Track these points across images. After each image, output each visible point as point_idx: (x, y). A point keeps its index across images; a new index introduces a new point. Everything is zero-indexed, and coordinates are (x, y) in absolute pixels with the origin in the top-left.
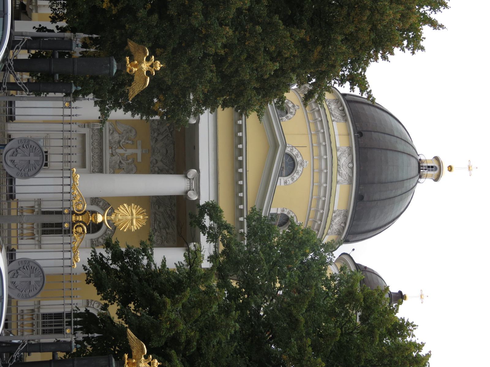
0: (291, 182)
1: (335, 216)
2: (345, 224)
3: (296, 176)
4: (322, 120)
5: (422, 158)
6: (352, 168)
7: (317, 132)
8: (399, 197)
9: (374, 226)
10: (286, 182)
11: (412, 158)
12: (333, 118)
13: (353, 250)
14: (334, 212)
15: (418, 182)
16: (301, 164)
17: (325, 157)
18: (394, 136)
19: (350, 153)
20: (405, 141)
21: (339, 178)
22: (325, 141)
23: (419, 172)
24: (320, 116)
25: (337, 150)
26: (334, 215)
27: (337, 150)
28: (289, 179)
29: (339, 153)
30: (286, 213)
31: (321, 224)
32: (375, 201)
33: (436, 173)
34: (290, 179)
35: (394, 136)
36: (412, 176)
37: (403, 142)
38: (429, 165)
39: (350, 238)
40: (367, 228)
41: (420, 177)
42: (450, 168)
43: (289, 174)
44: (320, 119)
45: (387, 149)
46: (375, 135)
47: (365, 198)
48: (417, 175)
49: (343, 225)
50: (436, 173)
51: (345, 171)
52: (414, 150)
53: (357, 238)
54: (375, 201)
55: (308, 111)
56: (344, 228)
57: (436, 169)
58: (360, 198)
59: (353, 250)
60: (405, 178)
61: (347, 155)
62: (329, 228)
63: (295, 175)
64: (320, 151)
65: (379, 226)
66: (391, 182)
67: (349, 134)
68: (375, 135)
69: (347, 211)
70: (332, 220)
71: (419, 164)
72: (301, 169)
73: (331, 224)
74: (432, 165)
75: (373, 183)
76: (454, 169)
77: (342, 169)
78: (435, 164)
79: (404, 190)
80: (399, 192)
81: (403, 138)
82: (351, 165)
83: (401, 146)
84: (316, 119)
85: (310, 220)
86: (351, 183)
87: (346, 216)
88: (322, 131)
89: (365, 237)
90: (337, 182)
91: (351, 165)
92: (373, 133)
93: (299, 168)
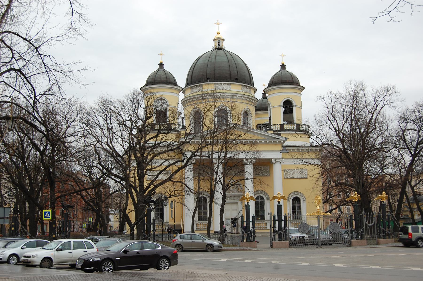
2: (247, 86)
6: (224, 83)
19: (218, 84)
21: (228, 89)
26: (243, 91)
31: (248, 98)
42: (218, 33)
46: (208, 72)
47: (237, 77)
49: (248, 87)
58: (237, 80)
66: (229, 65)
67: (208, 84)
68: (208, 72)
69: (242, 85)
70: (246, 92)
75: (230, 74)
78: (217, 41)
79: (232, 59)
82: (223, 84)
86: (230, 84)
90: (230, 90)
92: (207, 73)
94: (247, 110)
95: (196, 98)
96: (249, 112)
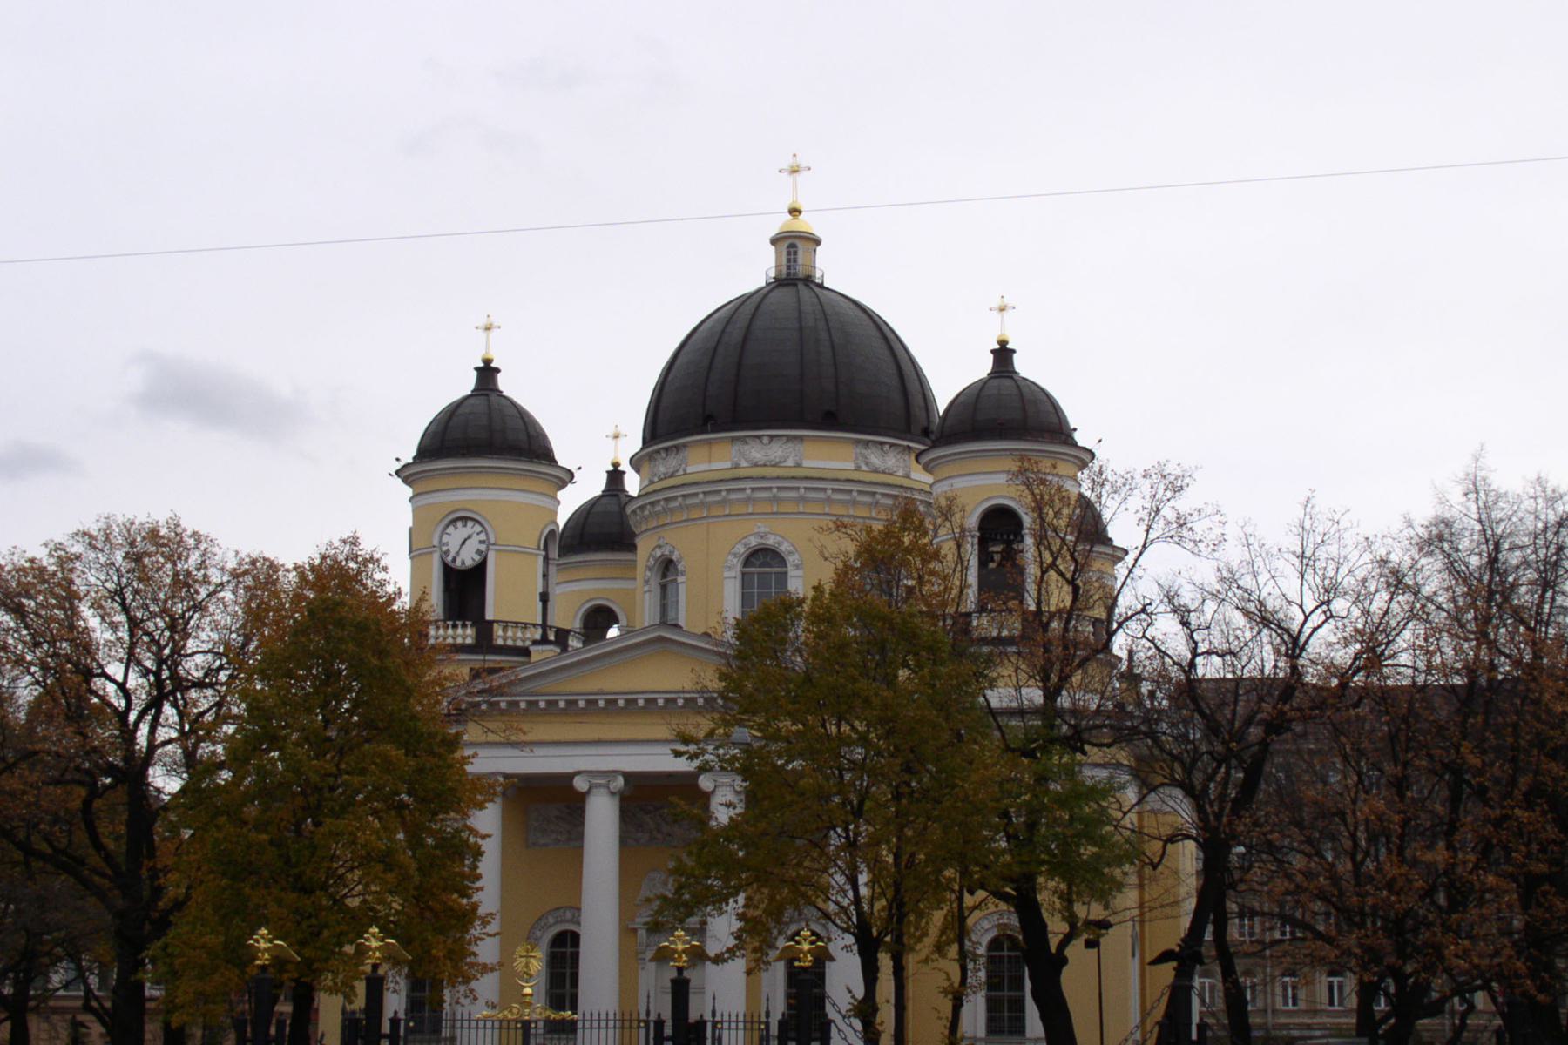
1: (867, 464)
2: (882, 443)
3: (784, 548)
5: (772, 274)
6: (772, 437)
7: (702, 504)
10: (797, 567)
11: (767, 301)
12: (681, 472)
16: (762, 537)
17: (748, 492)
19: (743, 440)
24: (675, 498)
26: (864, 468)
27: (737, 466)
28: (791, 560)
29: (744, 464)
33: (799, 244)
34: (791, 559)
37: (729, 328)
44: (680, 499)
45: (739, 364)
49: (886, 447)
51: (776, 451)
56: (892, 445)
57: (793, 246)
61: (746, 447)
63: (783, 548)
67: (709, 442)
69: (858, 442)
73: (884, 472)
77: (772, 457)
83: (736, 334)
86: (801, 438)
87: (867, 444)
91: (765, 440)
93: (770, 541)
95: (662, 503)
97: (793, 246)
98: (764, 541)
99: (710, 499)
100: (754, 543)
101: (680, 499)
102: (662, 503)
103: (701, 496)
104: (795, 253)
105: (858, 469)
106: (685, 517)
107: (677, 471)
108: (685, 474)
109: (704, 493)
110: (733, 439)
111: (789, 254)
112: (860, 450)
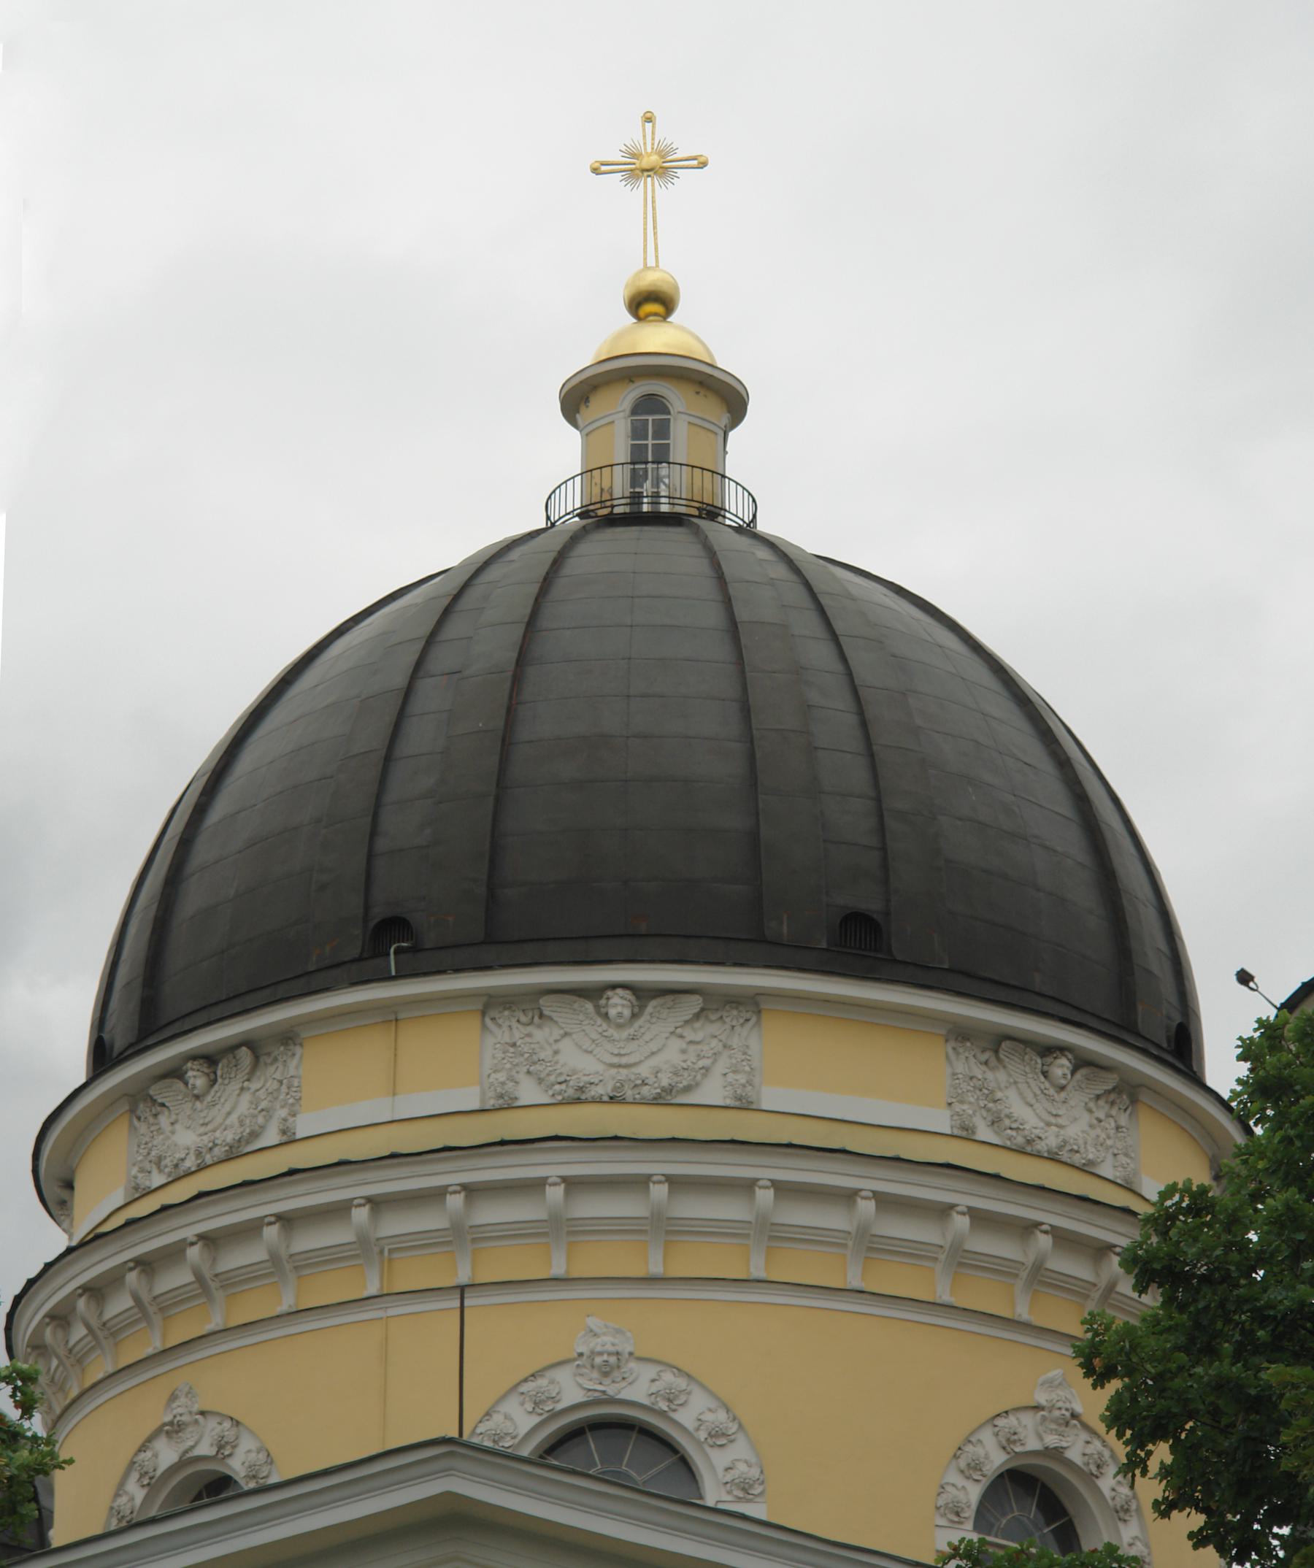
0: (739, 1450)
1: (995, 1122)
2: (1050, 1050)
4: (281, 1218)
5: (572, 499)
6: (642, 994)
7: (365, 1248)
8: (862, 661)
9: (1071, 843)
11: (574, 566)
12: (271, 1137)
13: (1244, 978)
14: (965, 1134)
15: (747, 530)
16: (606, 1371)
17: (555, 1194)
18: (408, 692)
20: (447, 612)
21: (712, 1091)
22: (438, 1195)
23: (674, 520)
24: (250, 1230)
25: (508, 1105)
26: (984, 1133)
27: (508, 1105)
29: (529, 1092)
30: (973, 1493)
31: (1055, 1232)
32: (882, 829)
33: (678, 398)
34: (720, 1459)
35: (408, 692)
36: (703, 566)
37: (455, 628)
38: (621, 452)
39: (1158, 1027)
40: (1083, 895)
41: (713, 513)
43: (685, 1463)
44: (271, 1232)
45: (506, 741)
47: (870, 903)
48: (697, 531)
49: (1061, 1067)
50: (678, 398)
52: (515, 554)
53: (1160, 968)
54: (882, 829)
55: (215, 1323)
56: (1083, 1062)
57: (650, 404)
59: (1244, 978)
60: (712, 616)
61: (541, 1034)
62: (1086, 1169)
63: (685, 1417)
64: (515, 1232)
65: (1063, 805)
67: (391, 1015)
69: (961, 1033)
71: (613, 521)
72: (649, 1371)
73: (1053, 1158)
74: (622, 427)
75: (754, 837)
76: (650, 280)
77: (644, 1071)
79: (806, 623)
80: (819, 654)
81: (425, 630)
82: (619, 1004)
84: (274, 1258)
85: (1023, 1311)
86: (750, 1003)
87: (998, 1042)
88: (361, 1215)
89: (1150, 915)
90: (744, 1105)
91: (619, 1004)
92: (382, 844)
94: (1056, 1453)
96: (1091, 1478)
97: (650, 404)
98: (611, 1390)
99: (396, 1225)
100: (572, 1395)
101: (271, 1232)
102: (194, 1253)
103: (361, 1215)
104: (663, 430)
105: (965, 1134)
106: (287, 1302)
107: (254, 1135)
108: (289, 1140)
109: (375, 1203)
110: (492, 1003)
111: (638, 431)
112: (968, 1064)
